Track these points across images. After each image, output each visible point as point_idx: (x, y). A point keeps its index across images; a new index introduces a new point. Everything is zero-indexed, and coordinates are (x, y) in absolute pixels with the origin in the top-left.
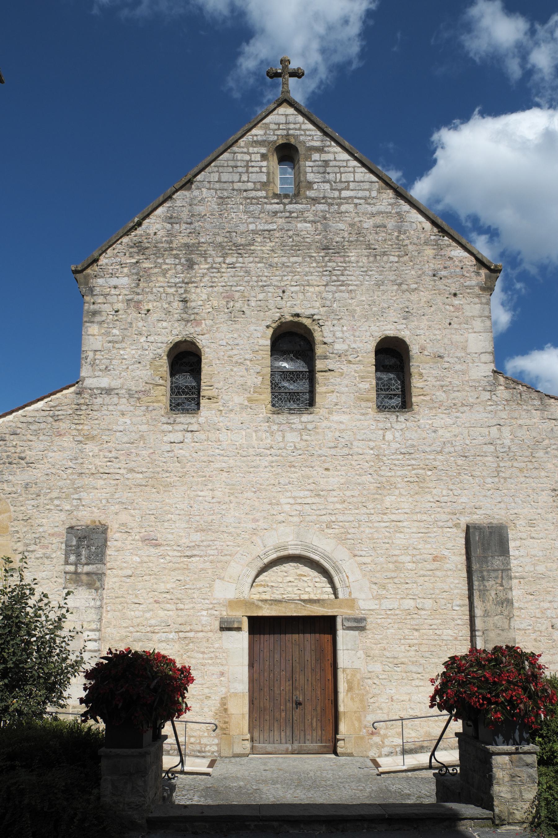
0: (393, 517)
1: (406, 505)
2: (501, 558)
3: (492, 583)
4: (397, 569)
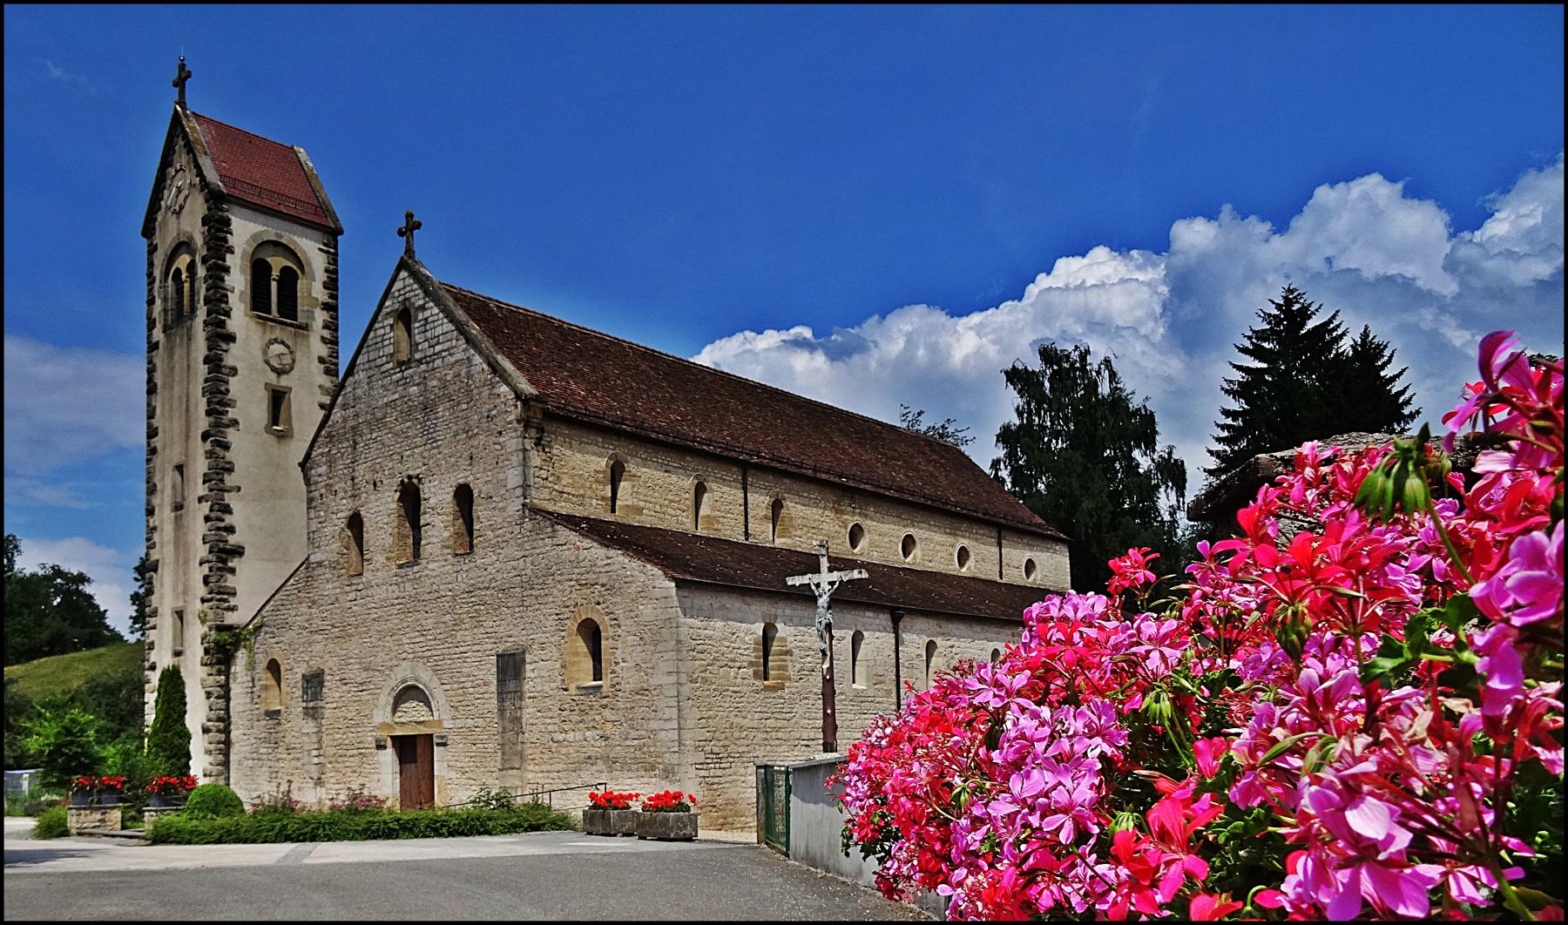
0: (462, 649)
1: (468, 638)
4: (465, 693)
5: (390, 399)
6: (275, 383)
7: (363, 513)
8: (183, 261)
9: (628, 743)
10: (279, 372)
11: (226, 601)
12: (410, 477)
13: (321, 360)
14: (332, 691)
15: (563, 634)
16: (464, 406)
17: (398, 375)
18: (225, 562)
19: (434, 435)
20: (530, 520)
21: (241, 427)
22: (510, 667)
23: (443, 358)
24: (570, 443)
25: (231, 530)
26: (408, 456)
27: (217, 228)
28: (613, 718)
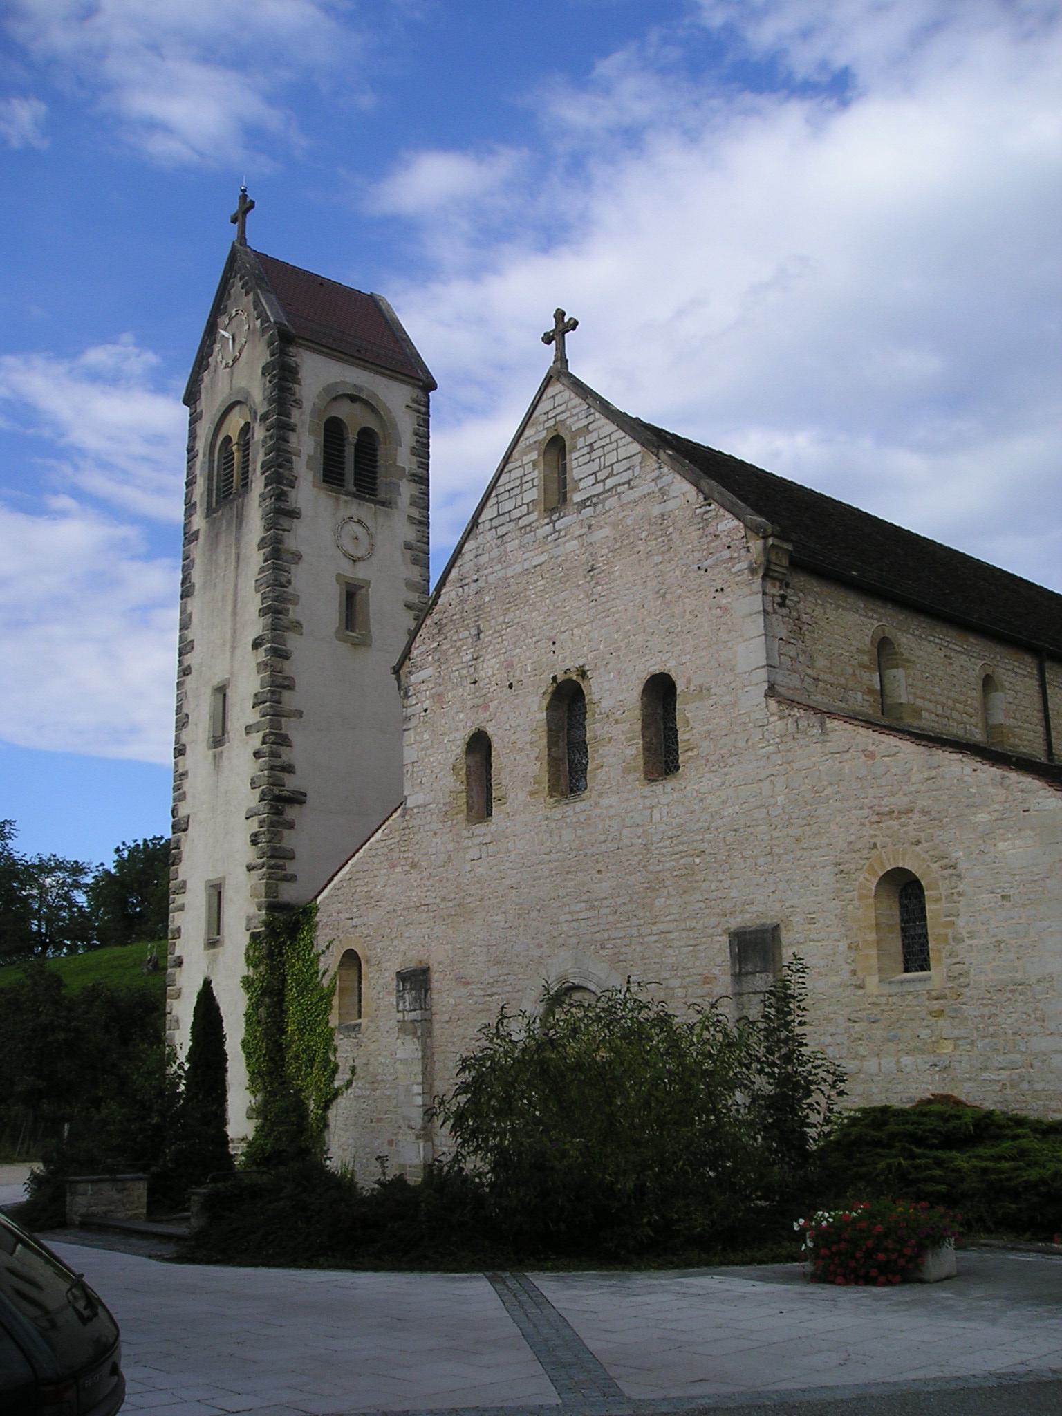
0: (662, 927)
1: (674, 910)
2: (763, 975)
6: (348, 574)
7: (490, 731)
8: (235, 422)
9: (986, 1075)
10: (355, 560)
13: (408, 547)
15: (849, 895)
16: (658, 559)
19: (608, 606)
20: (781, 718)
25: (289, 769)
28: (956, 1033)
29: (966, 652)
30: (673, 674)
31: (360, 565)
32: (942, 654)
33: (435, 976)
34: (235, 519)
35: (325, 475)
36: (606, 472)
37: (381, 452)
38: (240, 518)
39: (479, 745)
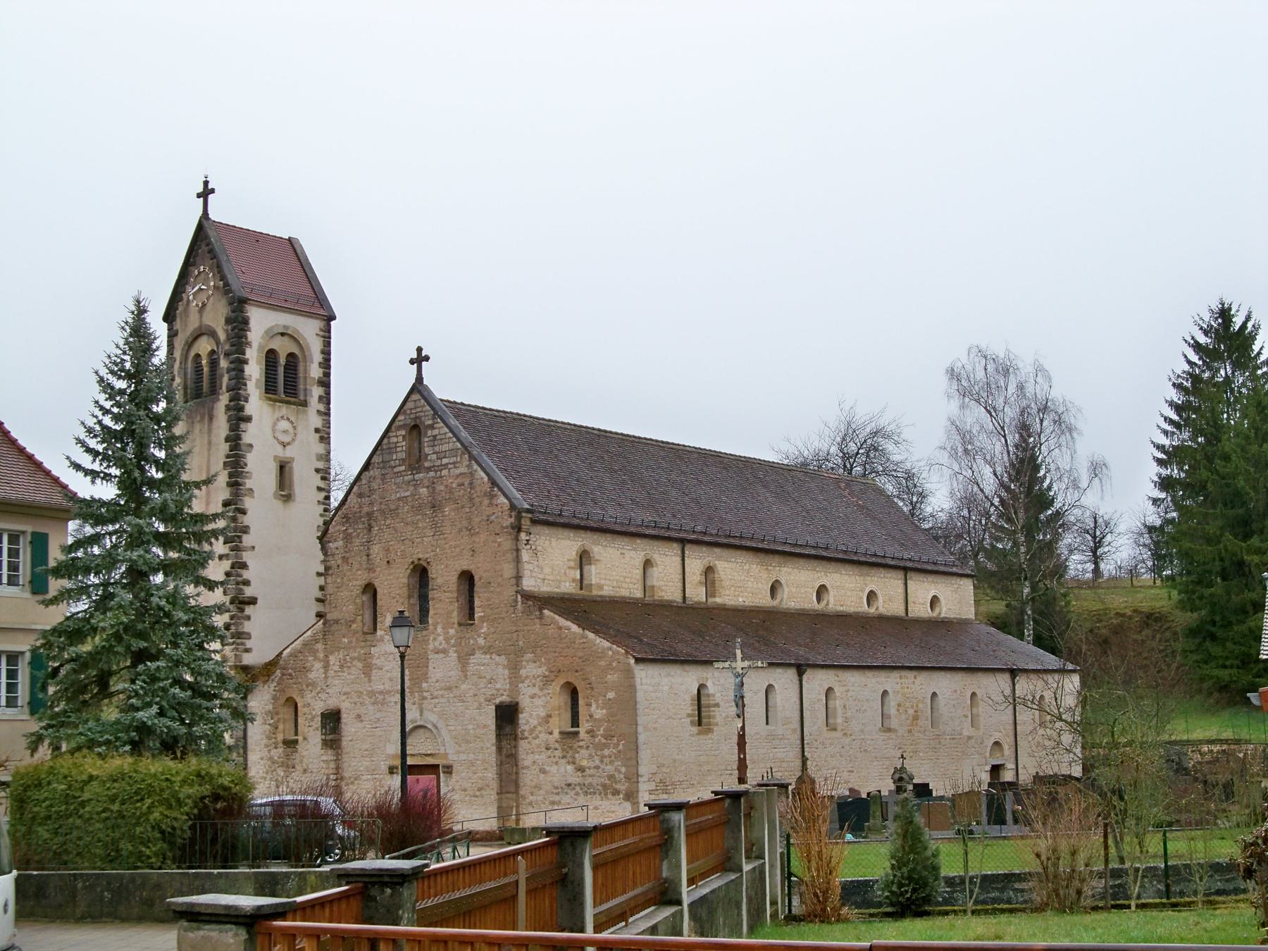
3: (505, 742)
5: (402, 495)
10: (284, 445)
11: (242, 644)
12: (419, 559)
14: (349, 727)
16: (468, 510)
17: (410, 477)
18: (242, 610)
19: (441, 529)
21: (255, 495)
22: (507, 715)
23: (449, 469)
24: (550, 540)
25: (247, 583)
26: (418, 543)
27: (238, 325)
29: (635, 549)
30: (473, 572)
31: (287, 447)
32: (619, 553)
33: (344, 716)
34: (207, 417)
35: (266, 389)
36: (443, 454)
37: (301, 368)
38: (211, 418)
39: (370, 590)
